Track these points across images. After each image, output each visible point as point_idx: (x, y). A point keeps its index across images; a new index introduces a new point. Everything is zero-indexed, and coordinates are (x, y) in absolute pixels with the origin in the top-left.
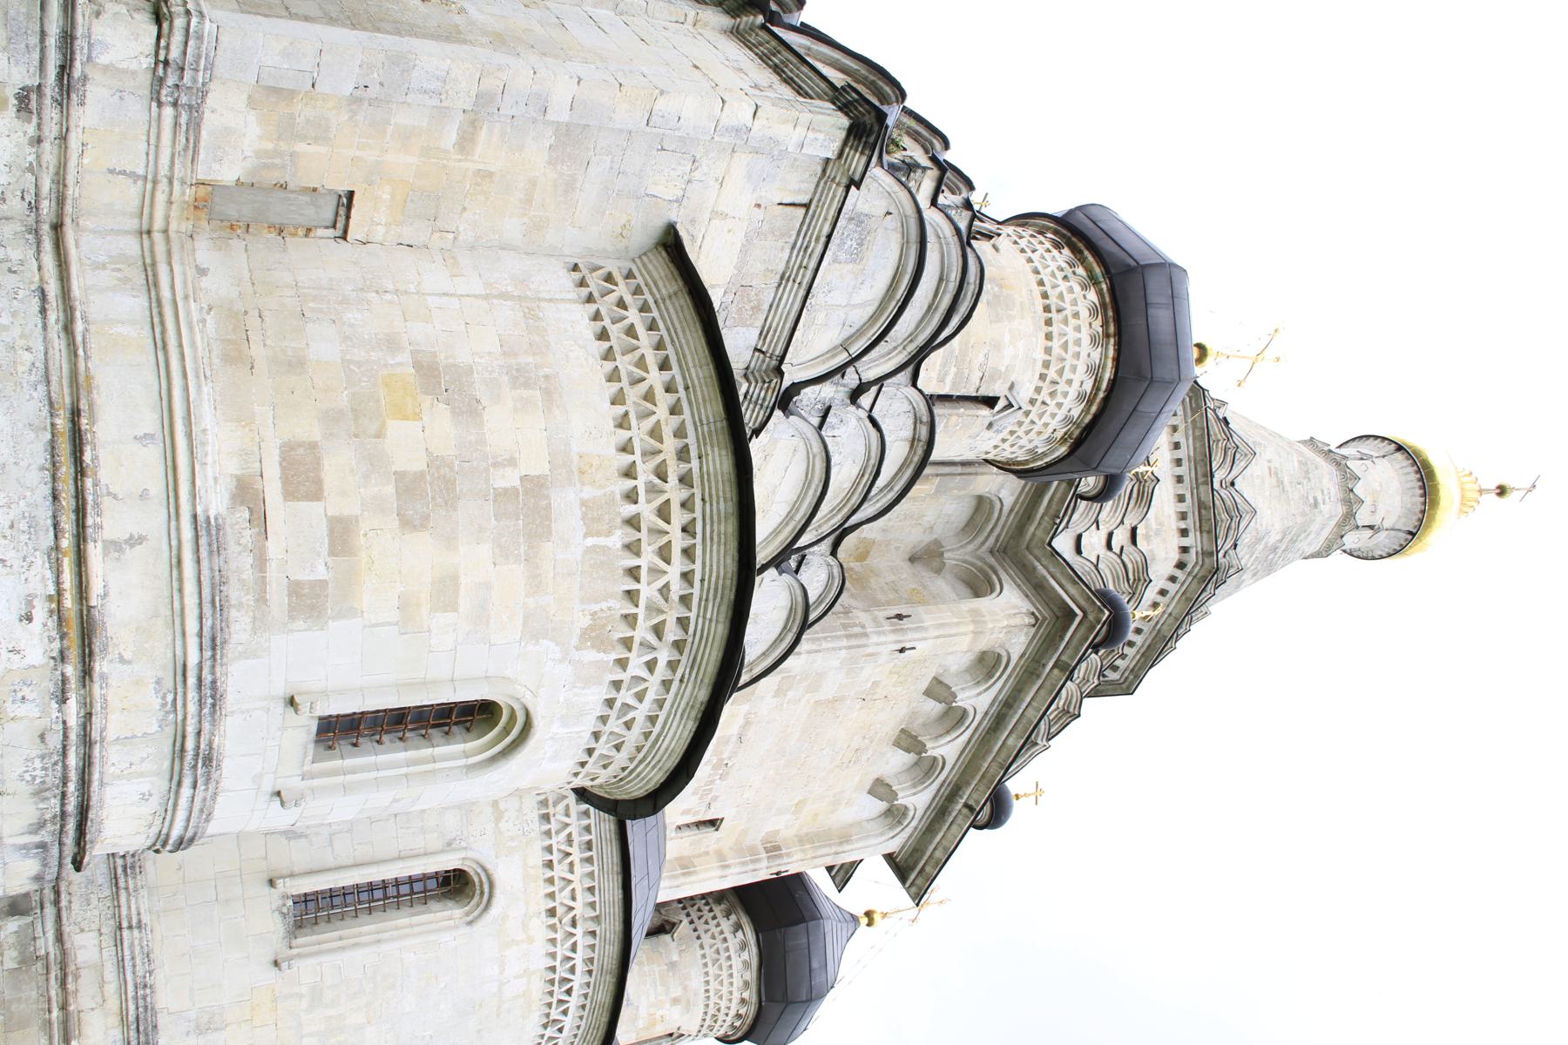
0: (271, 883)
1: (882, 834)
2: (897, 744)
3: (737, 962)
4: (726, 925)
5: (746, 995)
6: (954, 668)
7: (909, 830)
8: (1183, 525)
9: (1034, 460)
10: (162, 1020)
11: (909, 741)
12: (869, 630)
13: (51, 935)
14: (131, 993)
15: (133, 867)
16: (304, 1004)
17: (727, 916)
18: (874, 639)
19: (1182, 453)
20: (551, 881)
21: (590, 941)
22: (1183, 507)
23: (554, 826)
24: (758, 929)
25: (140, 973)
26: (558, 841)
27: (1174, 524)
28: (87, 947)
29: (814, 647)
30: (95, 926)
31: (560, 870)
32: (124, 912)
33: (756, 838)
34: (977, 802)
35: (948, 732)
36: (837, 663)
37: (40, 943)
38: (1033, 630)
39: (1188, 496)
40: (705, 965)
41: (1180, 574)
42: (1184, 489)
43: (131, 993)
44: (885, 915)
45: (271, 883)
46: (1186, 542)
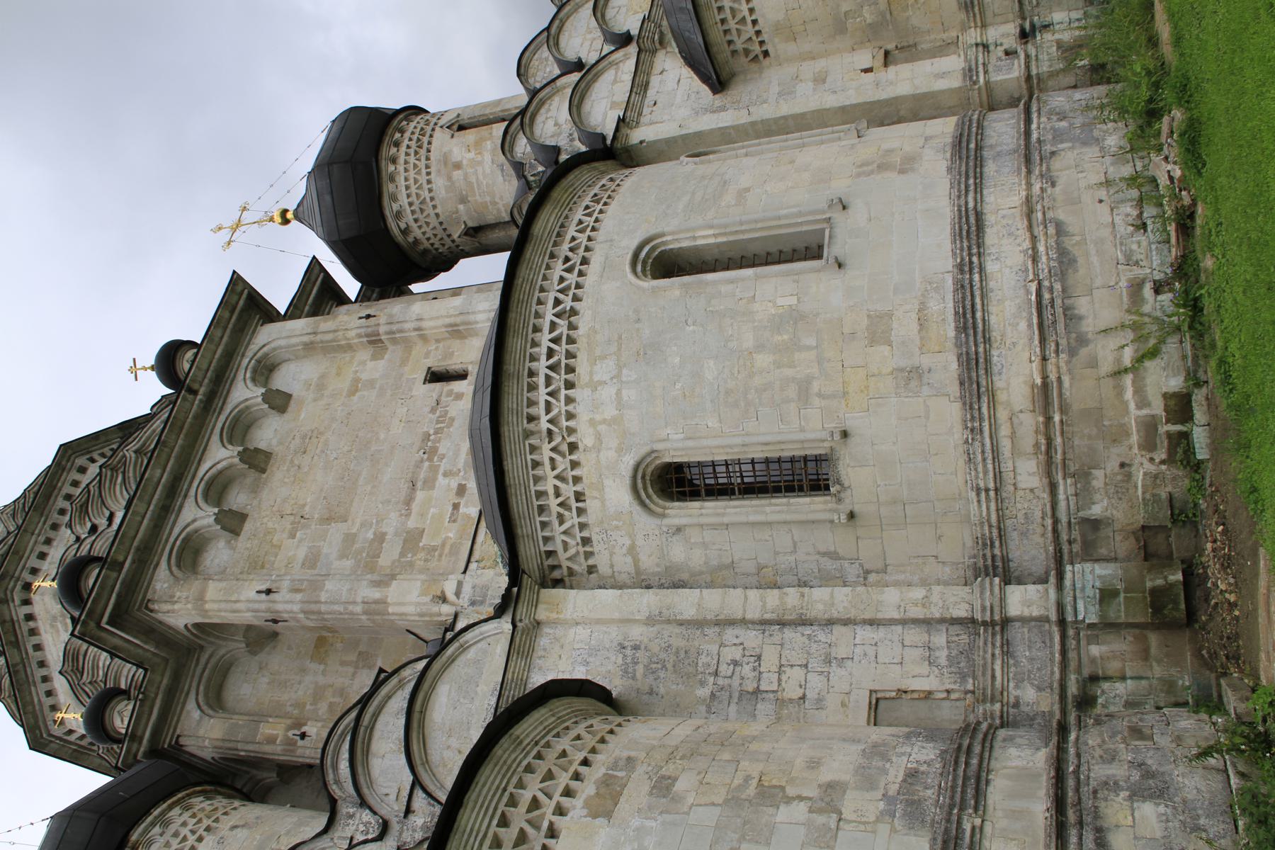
0: (852, 516)
1: (275, 349)
2: (268, 455)
3: (403, 200)
4: (417, 233)
5: (391, 168)
6: (222, 544)
7: (249, 354)
8: (31, 624)
9: (163, 813)
10: (955, 389)
11: (257, 461)
12: (301, 616)
13: (1061, 497)
14: (986, 424)
15: (985, 545)
16: (816, 386)
17: (416, 241)
18: (296, 608)
19: (43, 688)
20: (577, 480)
21: (533, 411)
22: (34, 640)
23: (578, 535)
24: (386, 230)
25: (977, 444)
26: (572, 520)
27: (42, 624)
28: (1026, 473)
29: (350, 607)
30: (1020, 493)
31: (568, 490)
32: (993, 506)
33: (393, 353)
34: (184, 399)
35: (220, 472)
36: (329, 585)
37: (1071, 490)
38: (149, 596)
39: (30, 651)
40: (432, 199)
41: (27, 576)
42: (35, 656)
43: (986, 424)
44: (272, 220)
45: (852, 516)
46: (26, 610)
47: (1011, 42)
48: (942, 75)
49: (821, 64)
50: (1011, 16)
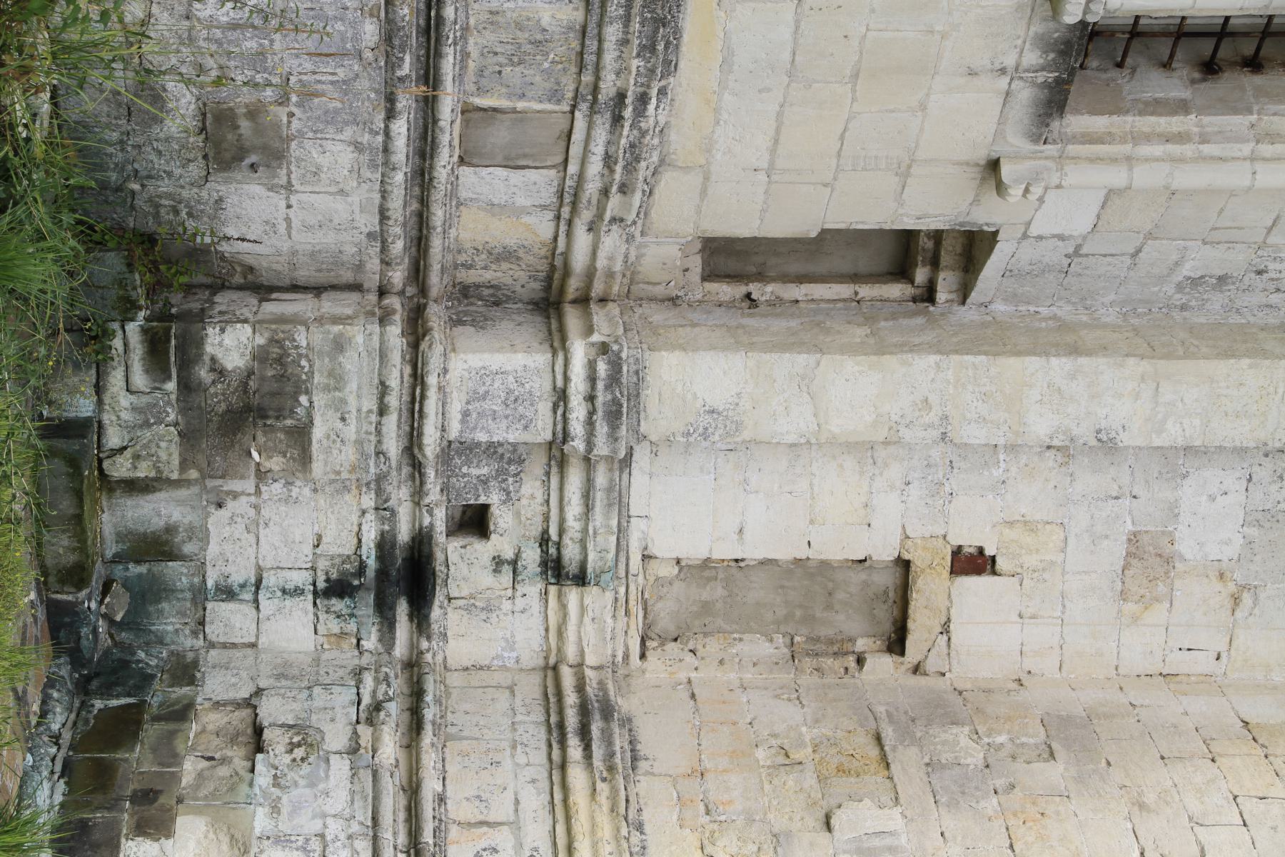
47: (464, 565)
48: (719, 435)
49: (1141, 646)
50: (454, 680)
